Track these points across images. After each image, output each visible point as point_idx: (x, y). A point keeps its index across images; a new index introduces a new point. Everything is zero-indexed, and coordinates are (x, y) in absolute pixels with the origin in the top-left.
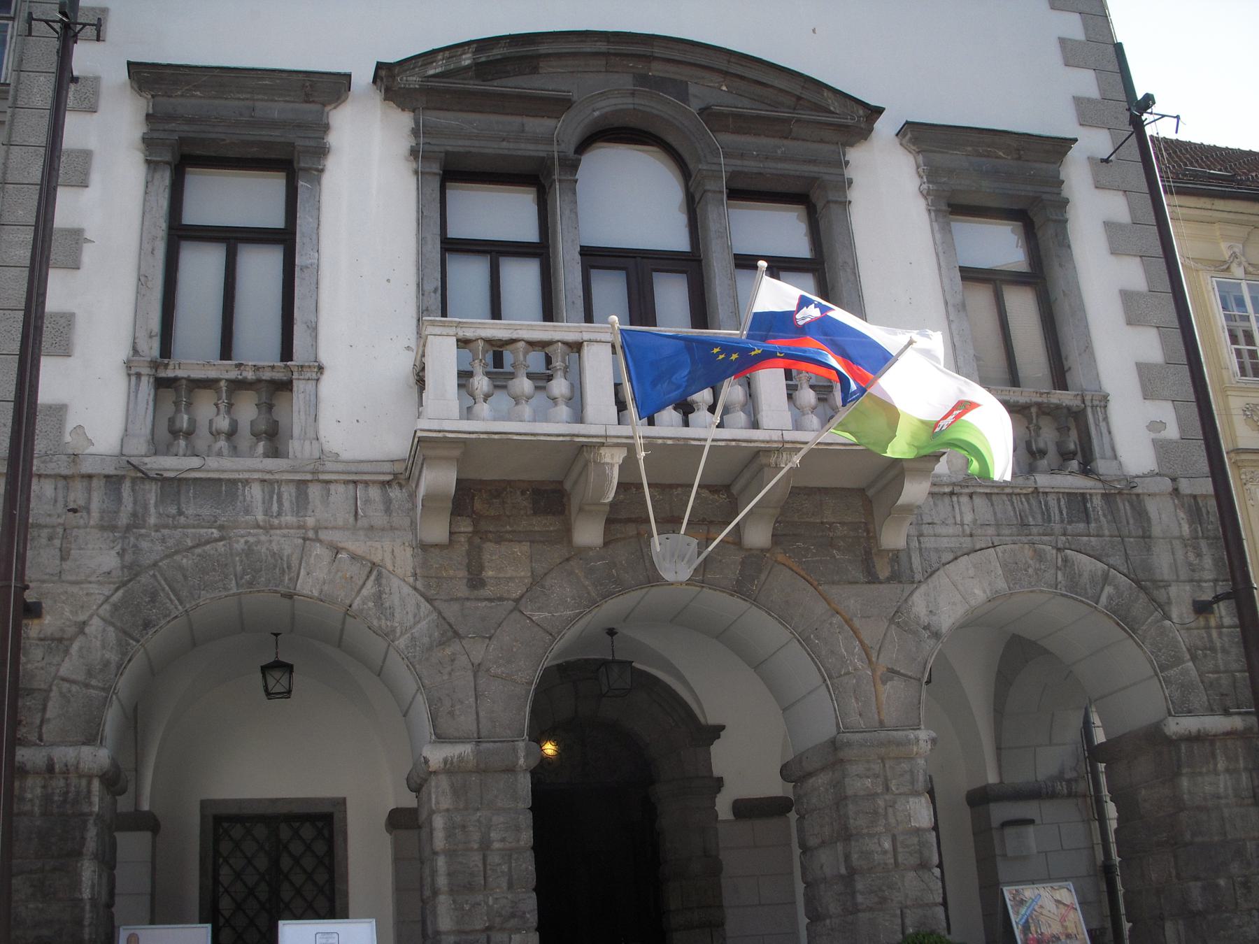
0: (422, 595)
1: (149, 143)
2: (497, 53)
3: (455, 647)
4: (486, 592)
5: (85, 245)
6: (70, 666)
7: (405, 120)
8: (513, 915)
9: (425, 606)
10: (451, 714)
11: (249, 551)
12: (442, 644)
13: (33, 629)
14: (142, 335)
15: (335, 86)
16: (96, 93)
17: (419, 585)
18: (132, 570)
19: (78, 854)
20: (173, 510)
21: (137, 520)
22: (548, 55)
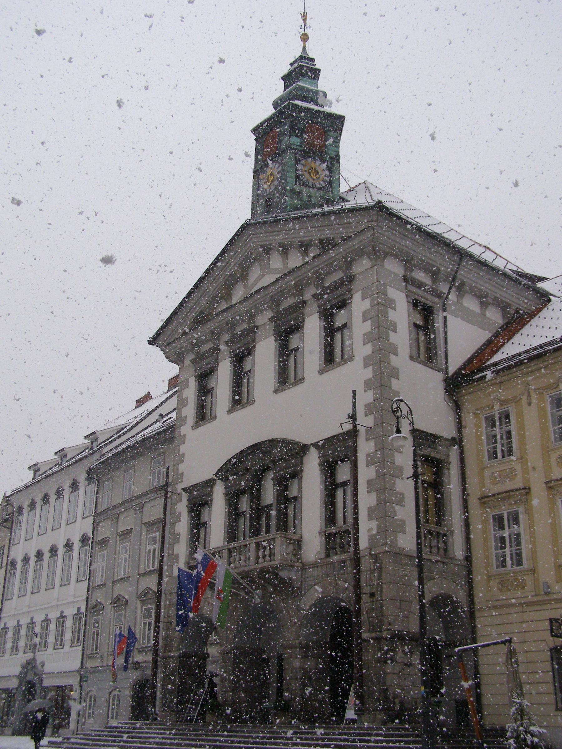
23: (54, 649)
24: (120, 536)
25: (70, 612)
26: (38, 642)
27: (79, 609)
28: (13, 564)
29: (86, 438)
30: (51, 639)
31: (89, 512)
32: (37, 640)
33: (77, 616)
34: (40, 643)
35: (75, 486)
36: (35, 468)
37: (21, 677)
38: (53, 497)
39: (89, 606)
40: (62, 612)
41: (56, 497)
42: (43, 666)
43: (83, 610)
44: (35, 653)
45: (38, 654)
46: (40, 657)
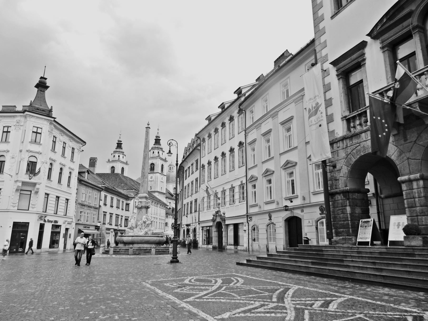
0: (395, 145)
1: (337, 75)
2: (391, 13)
3: (403, 155)
4: (408, 141)
5: (333, 100)
6: (341, 174)
7: (378, 42)
8: (422, 213)
9: (396, 148)
10: (404, 170)
11: (364, 147)
12: (400, 155)
13: (336, 170)
14: (343, 112)
15: (363, 44)
16: (329, 71)
17: (394, 144)
18: (347, 155)
19: (346, 206)
20: (351, 143)
21: (347, 147)
22: (404, 4)
23: (230, 205)
24: (263, 136)
25: (237, 184)
26: (220, 202)
27: (242, 182)
28: (203, 166)
29: (235, 93)
30: (228, 199)
31: (242, 129)
32: (220, 201)
33: (242, 186)
34: (222, 202)
35: (231, 119)
36: (209, 118)
37: (213, 220)
38: (220, 128)
39: (248, 179)
40: (232, 185)
41: (222, 128)
42: (224, 214)
43: (244, 182)
44: (219, 208)
45: (221, 208)
46: (222, 210)
